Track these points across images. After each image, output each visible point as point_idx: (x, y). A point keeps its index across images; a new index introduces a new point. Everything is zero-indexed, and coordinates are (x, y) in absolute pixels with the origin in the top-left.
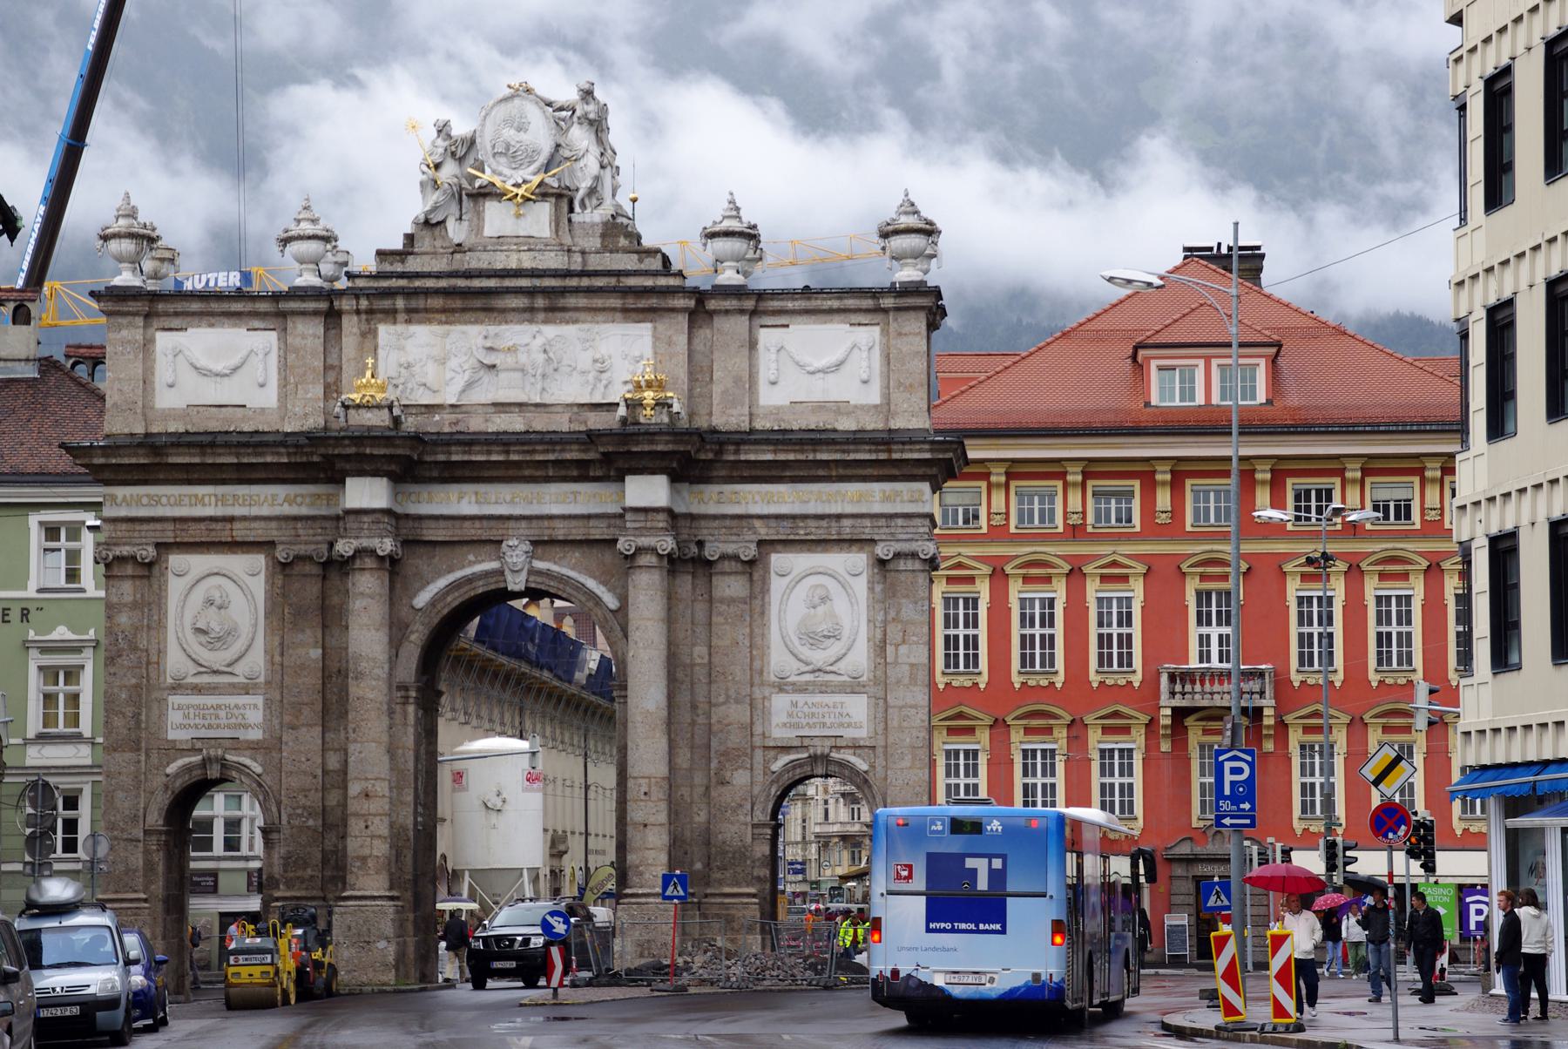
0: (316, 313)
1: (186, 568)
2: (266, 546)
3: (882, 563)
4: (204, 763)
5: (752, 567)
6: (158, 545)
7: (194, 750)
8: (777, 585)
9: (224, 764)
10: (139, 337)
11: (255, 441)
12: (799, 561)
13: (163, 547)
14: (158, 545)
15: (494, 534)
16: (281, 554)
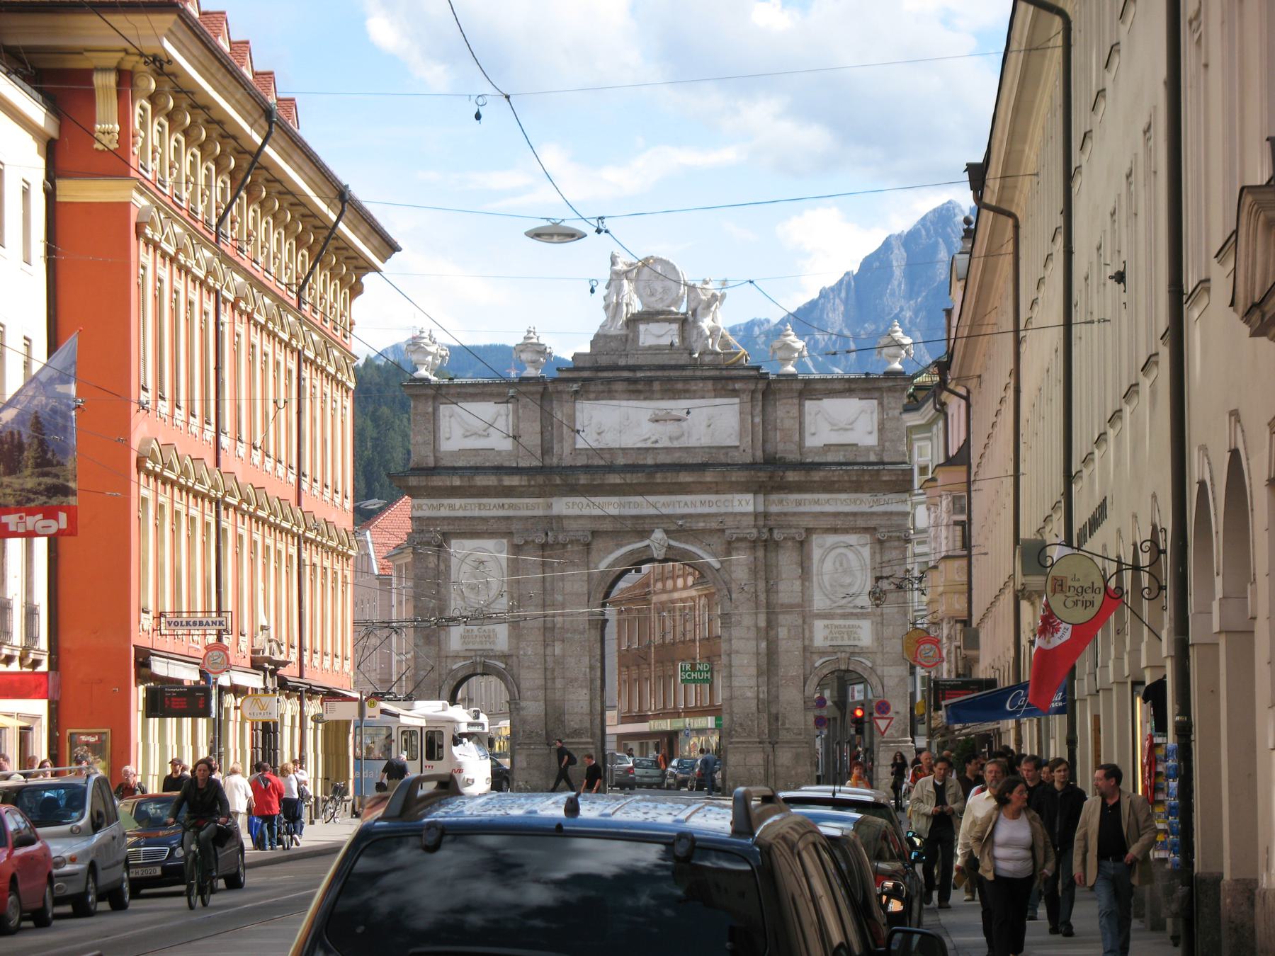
0: (537, 392)
1: (458, 548)
2: (508, 534)
3: (881, 542)
4: (474, 664)
5: (802, 545)
6: (444, 534)
7: (465, 658)
8: (816, 554)
9: (484, 665)
10: (430, 410)
11: (499, 470)
12: (831, 539)
13: (447, 536)
14: (444, 534)
15: (647, 527)
16: (518, 540)
